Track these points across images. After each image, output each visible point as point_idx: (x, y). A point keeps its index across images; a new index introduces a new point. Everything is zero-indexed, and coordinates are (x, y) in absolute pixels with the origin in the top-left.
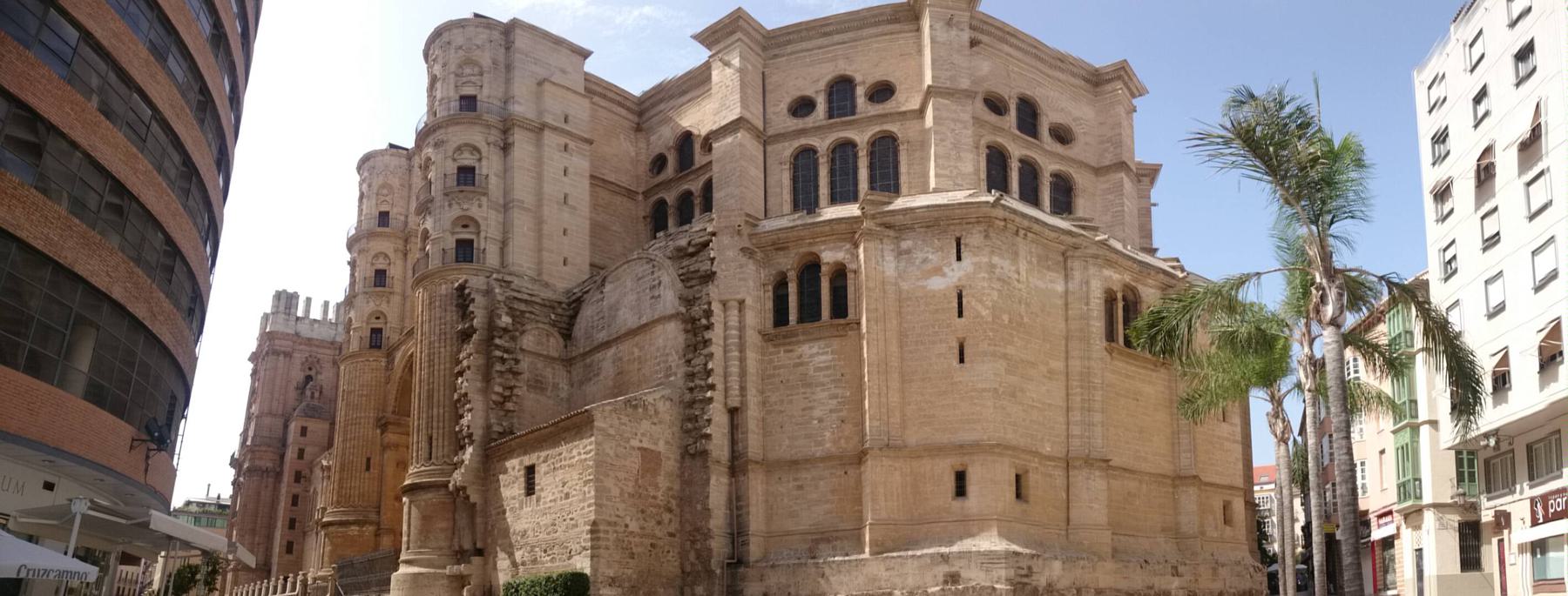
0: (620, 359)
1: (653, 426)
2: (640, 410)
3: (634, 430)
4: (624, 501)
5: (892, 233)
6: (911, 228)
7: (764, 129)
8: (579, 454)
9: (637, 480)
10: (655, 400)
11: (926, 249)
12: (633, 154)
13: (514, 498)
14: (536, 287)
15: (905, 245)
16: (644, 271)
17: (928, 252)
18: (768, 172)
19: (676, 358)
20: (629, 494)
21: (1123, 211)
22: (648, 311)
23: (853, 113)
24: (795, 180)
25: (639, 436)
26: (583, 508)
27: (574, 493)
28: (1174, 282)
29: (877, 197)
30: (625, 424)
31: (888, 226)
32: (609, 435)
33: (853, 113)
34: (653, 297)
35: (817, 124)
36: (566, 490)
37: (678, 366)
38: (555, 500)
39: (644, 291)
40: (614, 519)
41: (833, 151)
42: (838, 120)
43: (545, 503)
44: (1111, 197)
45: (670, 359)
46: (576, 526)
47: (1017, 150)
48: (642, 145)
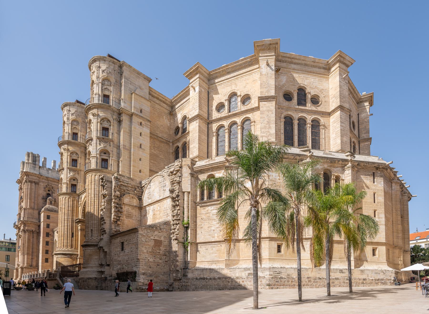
1: (159, 233)
2: (154, 228)
3: (152, 234)
9: (153, 248)
13: (118, 251)
14: (129, 181)
16: (162, 180)
19: (169, 210)
20: (150, 252)
22: (162, 195)
25: (154, 236)
30: (149, 232)
34: (163, 190)
36: (131, 250)
37: (170, 213)
38: (129, 252)
39: (161, 187)
40: (144, 258)
43: (126, 253)
45: (168, 211)
46: (134, 259)
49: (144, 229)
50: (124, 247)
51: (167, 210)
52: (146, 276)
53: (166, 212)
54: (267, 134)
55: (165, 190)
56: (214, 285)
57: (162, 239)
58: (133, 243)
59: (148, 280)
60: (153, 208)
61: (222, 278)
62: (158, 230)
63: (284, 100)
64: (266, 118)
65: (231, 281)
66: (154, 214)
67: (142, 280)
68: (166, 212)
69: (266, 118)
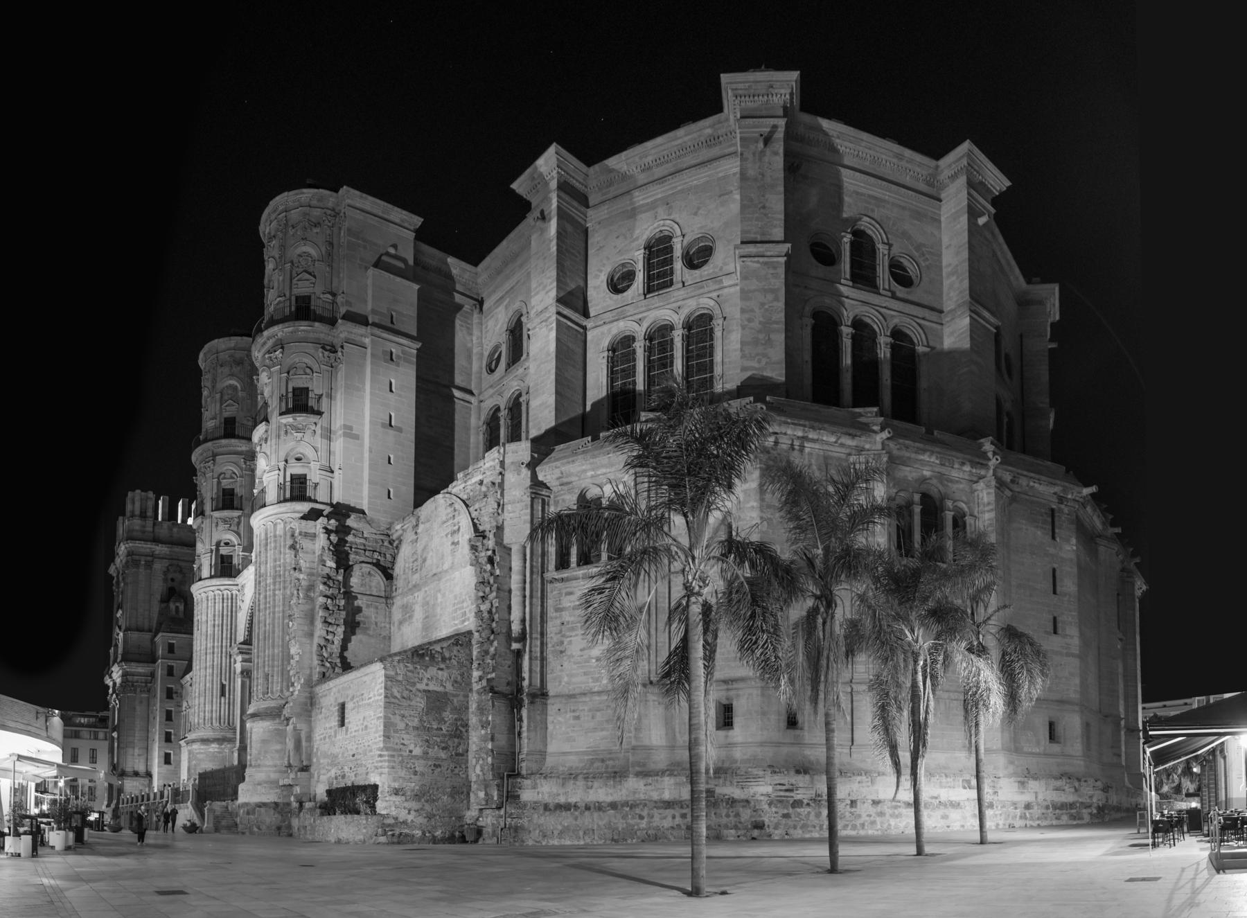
0: (428, 603)
1: (440, 672)
2: (427, 658)
3: (420, 676)
4: (408, 733)
8: (375, 696)
10: (442, 648)
16: (447, 514)
19: (470, 602)
25: (425, 681)
26: (376, 738)
27: (371, 726)
32: (397, 681)
34: (453, 543)
36: (365, 723)
37: (470, 611)
38: (358, 730)
39: (447, 535)
43: (351, 733)
45: (465, 605)
46: (371, 751)
49: (399, 662)
50: (346, 716)
51: (463, 602)
52: (403, 798)
53: (460, 609)
55: (458, 543)
56: (599, 826)
57: (449, 687)
58: (369, 704)
59: (409, 811)
60: (424, 599)
61: (623, 806)
62: (437, 663)
65: (649, 814)
66: (427, 617)
67: (393, 809)
68: (460, 609)
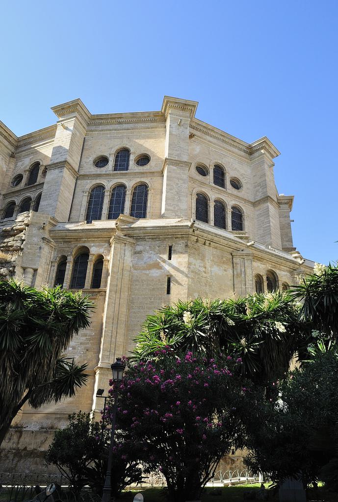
5: (131, 240)
6: (143, 239)
7: (78, 171)
11: (150, 252)
12: (5, 169)
15: (138, 248)
17: (151, 254)
18: (75, 195)
21: (270, 226)
23: (127, 169)
24: (90, 203)
28: (296, 266)
29: (131, 219)
31: (130, 236)
33: (127, 169)
35: (107, 173)
41: (114, 189)
42: (119, 172)
44: (262, 219)
47: (213, 194)
48: (12, 166)
54: (174, 208)
63: (197, 172)
64: (175, 186)
69: (175, 186)
